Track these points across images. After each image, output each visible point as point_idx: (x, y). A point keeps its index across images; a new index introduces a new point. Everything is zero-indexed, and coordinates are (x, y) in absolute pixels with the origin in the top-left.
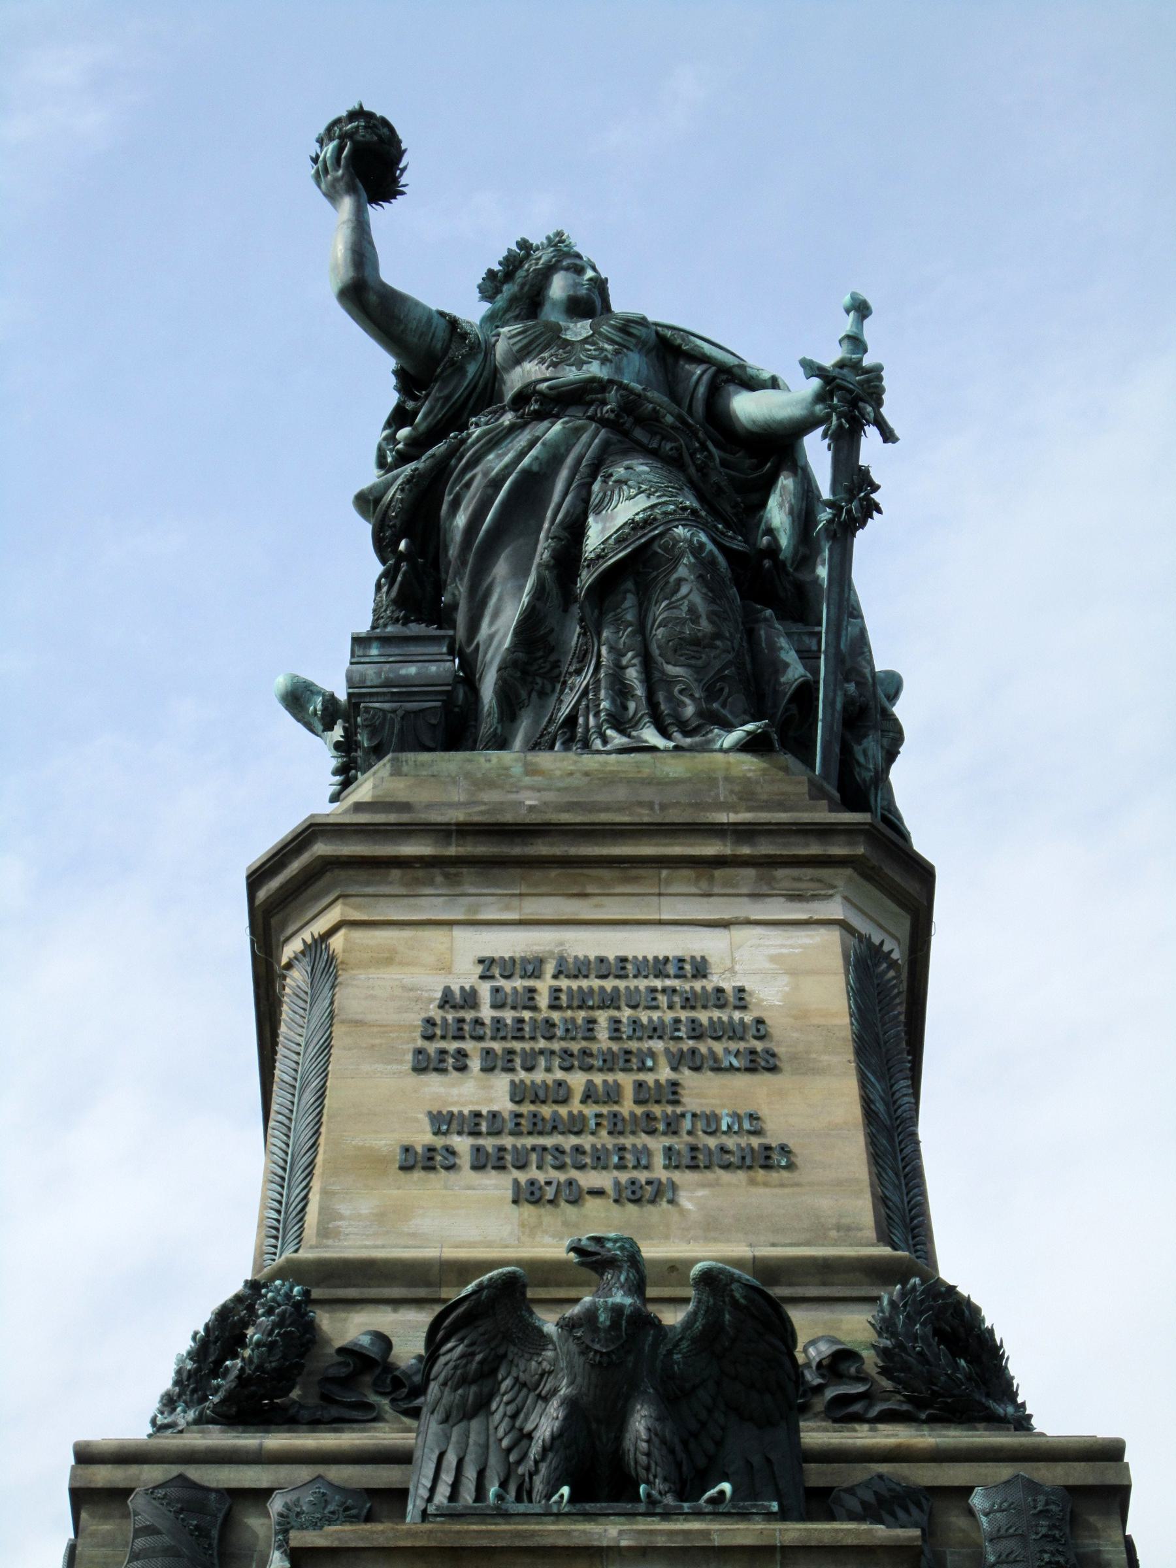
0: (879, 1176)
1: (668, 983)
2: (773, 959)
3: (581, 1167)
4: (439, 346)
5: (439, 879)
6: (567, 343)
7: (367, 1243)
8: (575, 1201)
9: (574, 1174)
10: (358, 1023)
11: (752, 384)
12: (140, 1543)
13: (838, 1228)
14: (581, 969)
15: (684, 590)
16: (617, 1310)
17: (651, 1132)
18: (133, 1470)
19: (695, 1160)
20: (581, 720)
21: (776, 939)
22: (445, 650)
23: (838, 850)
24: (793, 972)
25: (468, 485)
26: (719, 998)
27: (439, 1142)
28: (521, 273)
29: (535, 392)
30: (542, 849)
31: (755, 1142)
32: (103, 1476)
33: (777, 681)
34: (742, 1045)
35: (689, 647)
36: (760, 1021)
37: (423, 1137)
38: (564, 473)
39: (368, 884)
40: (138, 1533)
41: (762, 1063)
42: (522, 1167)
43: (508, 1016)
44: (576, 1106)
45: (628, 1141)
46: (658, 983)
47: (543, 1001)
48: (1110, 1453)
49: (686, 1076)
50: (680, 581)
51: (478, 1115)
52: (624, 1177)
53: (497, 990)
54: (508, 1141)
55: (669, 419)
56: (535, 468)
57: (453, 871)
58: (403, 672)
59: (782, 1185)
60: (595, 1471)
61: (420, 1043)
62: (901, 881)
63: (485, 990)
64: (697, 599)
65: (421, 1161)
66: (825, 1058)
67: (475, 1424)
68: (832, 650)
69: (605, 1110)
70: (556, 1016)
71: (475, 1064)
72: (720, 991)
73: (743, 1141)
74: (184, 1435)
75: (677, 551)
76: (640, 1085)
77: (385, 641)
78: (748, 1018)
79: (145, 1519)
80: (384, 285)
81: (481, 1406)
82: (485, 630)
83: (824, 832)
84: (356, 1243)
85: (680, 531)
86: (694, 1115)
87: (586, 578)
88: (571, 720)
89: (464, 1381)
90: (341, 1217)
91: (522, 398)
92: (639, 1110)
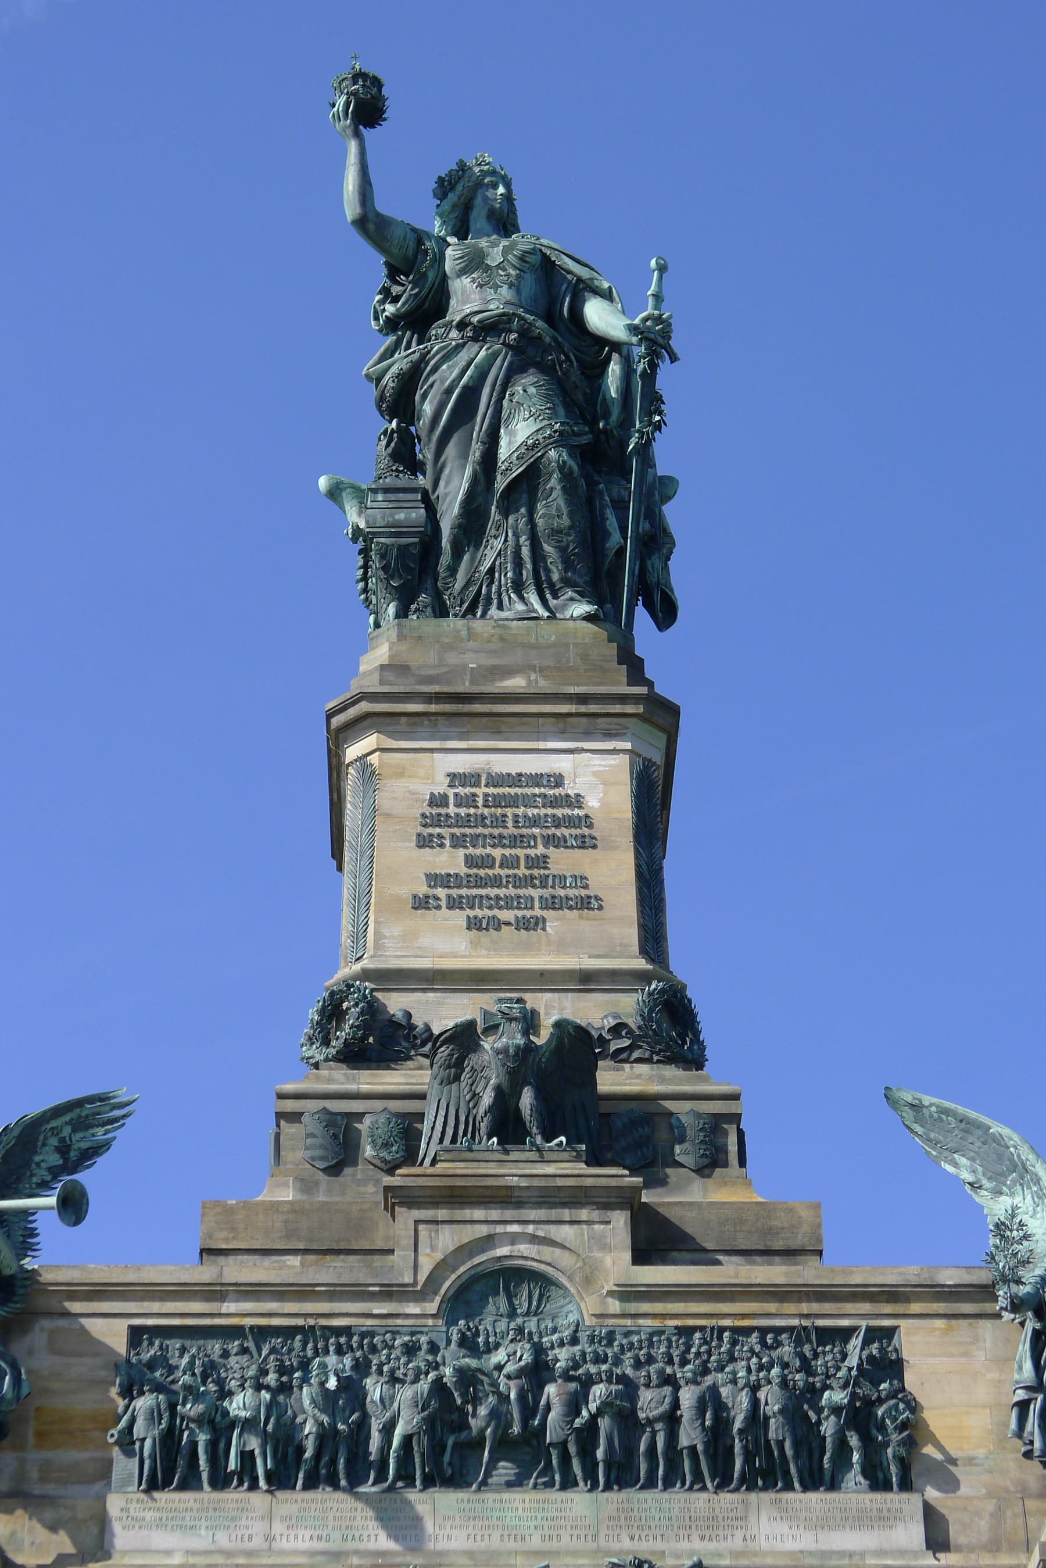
0: (642, 912)
1: (543, 790)
2: (595, 774)
3: (500, 908)
4: (411, 253)
5: (426, 722)
6: (488, 268)
7: (398, 953)
8: (498, 929)
9: (496, 912)
10: (388, 815)
11: (597, 292)
12: (309, 1141)
13: (621, 945)
14: (498, 780)
15: (554, 495)
16: (518, 1047)
17: (534, 886)
18: (303, 1102)
19: (552, 904)
20: (497, 575)
21: (597, 760)
22: (419, 498)
23: (630, 709)
24: (605, 783)
25: (431, 386)
26: (568, 801)
27: (431, 892)
28: (459, 188)
29: (471, 323)
30: (478, 708)
31: (584, 892)
32: (290, 1106)
33: (604, 545)
34: (578, 831)
35: (555, 533)
36: (587, 816)
37: (423, 889)
38: (486, 391)
39: (389, 725)
40: (308, 1136)
41: (586, 843)
42: (472, 908)
43: (463, 811)
44: (497, 871)
45: (521, 892)
46: (537, 791)
47: (480, 802)
48: (735, 1097)
49: (552, 851)
50: (552, 489)
51: (449, 875)
52: (520, 913)
53: (456, 795)
54: (464, 892)
55: (548, 339)
56: (471, 384)
57: (433, 718)
58: (397, 517)
59: (595, 919)
60: (507, 1127)
61: (420, 829)
62: (662, 715)
63: (451, 793)
64: (561, 502)
65: (422, 903)
66: (619, 839)
67: (454, 1086)
68: (634, 534)
69: (511, 872)
70: (486, 811)
71: (447, 843)
72: (568, 796)
73: (576, 892)
74: (324, 1073)
75: (550, 469)
76: (527, 857)
77: (387, 490)
78: (581, 813)
79: (311, 1129)
80: (378, 215)
81: (457, 1078)
82: (441, 489)
83: (623, 699)
84: (396, 959)
85: (552, 453)
86: (554, 876)
87: (501, 483)
88: (491, 571)
89: (449, 1067)
90: (385, 937)
91: (462, 325)
92: (527, 872)
